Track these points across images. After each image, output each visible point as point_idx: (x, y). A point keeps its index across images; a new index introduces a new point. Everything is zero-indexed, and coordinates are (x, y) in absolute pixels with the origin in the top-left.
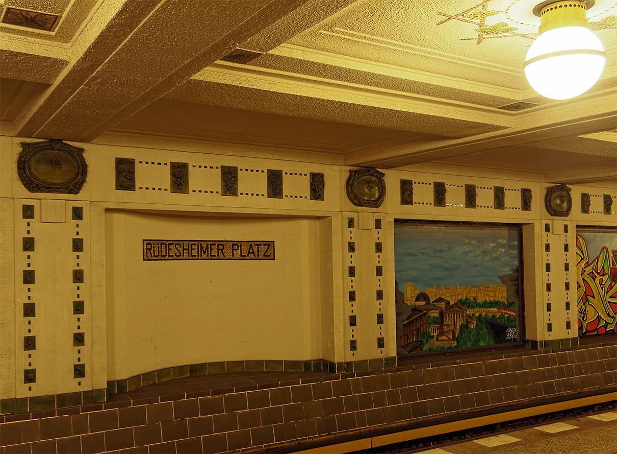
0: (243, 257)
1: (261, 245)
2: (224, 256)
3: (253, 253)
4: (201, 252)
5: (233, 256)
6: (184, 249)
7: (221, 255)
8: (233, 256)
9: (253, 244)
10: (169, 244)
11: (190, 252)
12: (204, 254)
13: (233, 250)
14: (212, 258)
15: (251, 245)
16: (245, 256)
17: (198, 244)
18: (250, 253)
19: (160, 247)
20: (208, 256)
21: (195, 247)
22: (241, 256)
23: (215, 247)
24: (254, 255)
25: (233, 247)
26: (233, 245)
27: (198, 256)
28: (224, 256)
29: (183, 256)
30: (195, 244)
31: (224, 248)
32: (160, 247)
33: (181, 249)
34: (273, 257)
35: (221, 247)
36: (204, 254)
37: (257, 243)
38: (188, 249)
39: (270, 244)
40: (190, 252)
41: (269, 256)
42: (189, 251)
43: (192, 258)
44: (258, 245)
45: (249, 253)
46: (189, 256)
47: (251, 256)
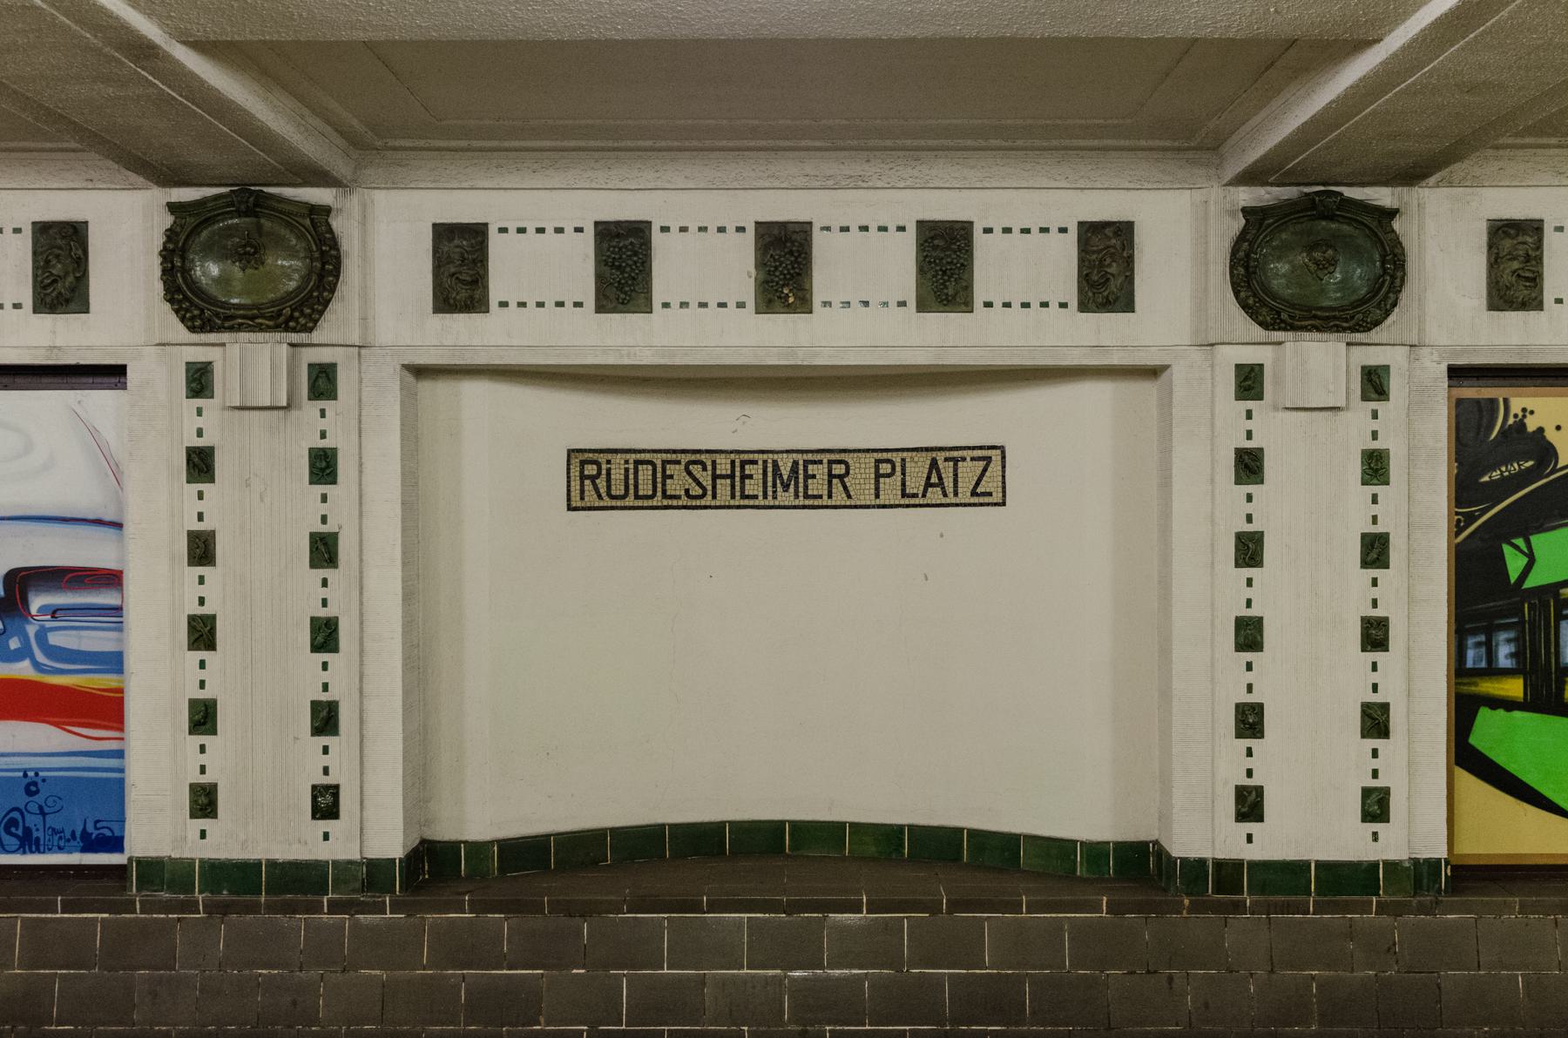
0: (908, 500)
1: (964, 459)
2: (849, 497)
3: (941, 484)
4: (774, 485)
5: (877, 496)
6: (715, 477)
7: (839, 497)
8: (877, 496)
9: (940, 456)
10: (664, 463)
11: (738, 484)
12: (786, 487)
13: (878, 476)
14: (812, 503)
15: (934, 464)
16: (915, 496)
17: (765, 462)
18: (933, 485)
19: (631, 471)
20: (797, 496)
21: (755, 471)
22: (904, 495)
23: (820, 471)
24: (943, 489)
25: (877, 468)
26: (878, 462)
27: (765, 496)
28: (849, 497)
29: (714, 497)
30: (754, 462)
31: (847, 473)
32: (631, 471)
33: (706, 480)
34: (997, 497)
35: (839, 469)
36: (786, 487)
37: (955, 454)
38: (732, 476)
39: (990, 456)
40: (738, 484)
41: (990, 494)
42: (733, 487)
43: (745, 501)
44: (956, 461)
45: (928, 484)
46: (733, 496)
47: (934, 495)
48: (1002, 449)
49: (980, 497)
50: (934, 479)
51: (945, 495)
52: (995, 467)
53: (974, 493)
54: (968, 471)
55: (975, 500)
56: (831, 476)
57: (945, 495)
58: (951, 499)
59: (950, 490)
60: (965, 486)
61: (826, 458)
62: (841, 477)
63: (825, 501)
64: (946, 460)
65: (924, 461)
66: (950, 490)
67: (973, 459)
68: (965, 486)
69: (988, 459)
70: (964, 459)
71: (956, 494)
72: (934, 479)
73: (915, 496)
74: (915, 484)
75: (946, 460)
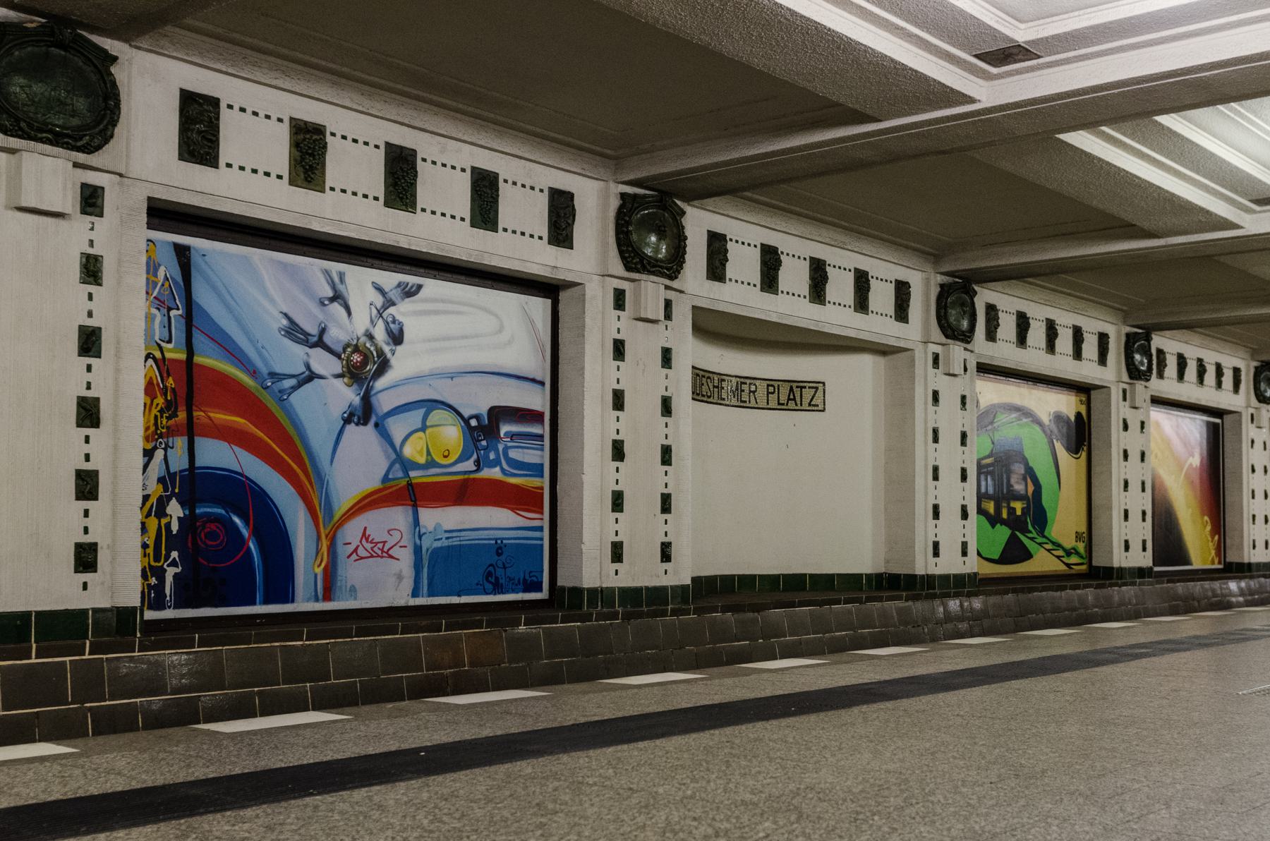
0: (781, 407)
1: (805, 387)
3: (794, 399)
5: (768, 403)
8: (768, 403)
13: (768, 393)
16: (783, 404)
18: (791, 400)
22: (779, 404)
25: (768, 389)
26: (768, 386)
31: (756, 391)
34: (821, 407)
35: (753, 388)
39: (817, 386)
41: (818, 406)
44: (802, 388)
45: (789, 399)
47: (792, 405)
48: (824, 383)
49: (813, 407)
50: (792, 397)
51: (796, 405)
52: (820, 393)
53: (810, 405)
54: (808, 394)
55: (810, 408)
56: (750, 391)
57: (796, 405)
58: (799, 407)
59: (799, 403)
60: (806, 402)
61: (748, 381)
62: (754, 392)
63: (747, 405)
64: (797, 387)
65: (787, 386)
66: (799, 403)
67: (809, 388)
68: (806, 402)
69: (817, 388)
70: (805, 387)
71: (801, 405)
72: (792, 397)
73: (783, 404)
74: (783, 399)
75: (797, 387)
